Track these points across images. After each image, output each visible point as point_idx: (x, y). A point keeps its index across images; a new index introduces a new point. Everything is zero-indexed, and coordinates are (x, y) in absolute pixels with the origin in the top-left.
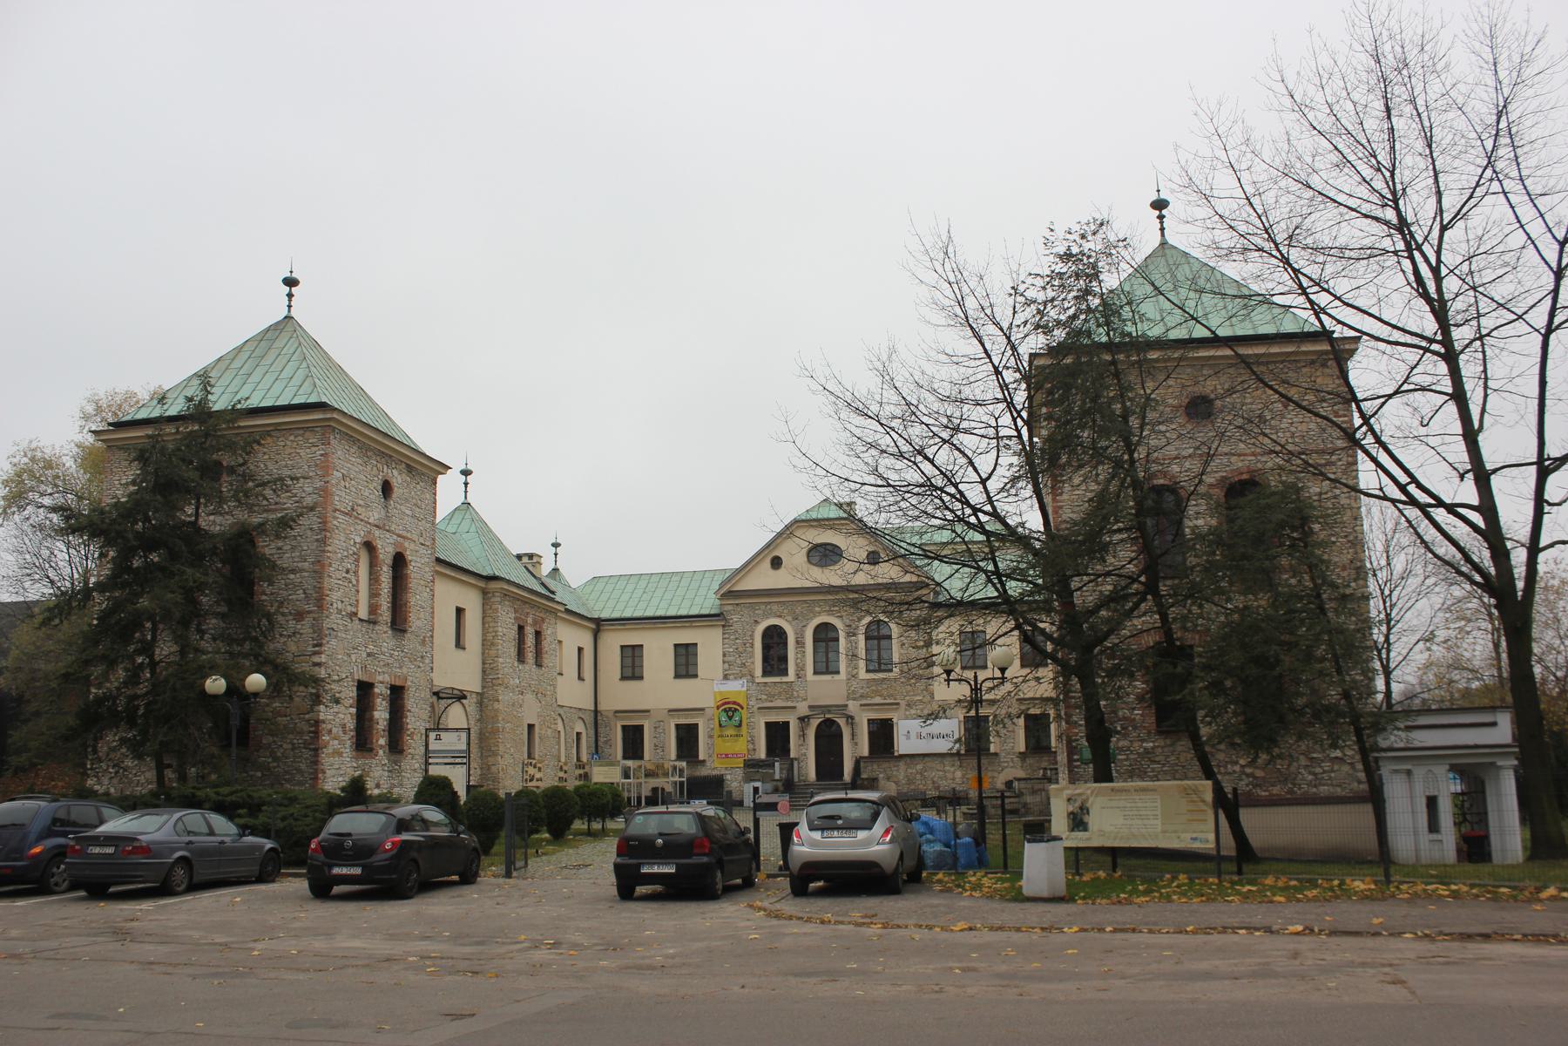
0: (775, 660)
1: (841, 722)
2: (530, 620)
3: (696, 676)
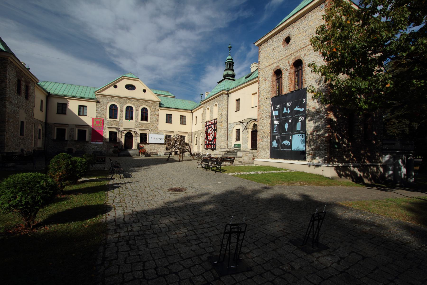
2: (23, 79)
3: (86, 116)
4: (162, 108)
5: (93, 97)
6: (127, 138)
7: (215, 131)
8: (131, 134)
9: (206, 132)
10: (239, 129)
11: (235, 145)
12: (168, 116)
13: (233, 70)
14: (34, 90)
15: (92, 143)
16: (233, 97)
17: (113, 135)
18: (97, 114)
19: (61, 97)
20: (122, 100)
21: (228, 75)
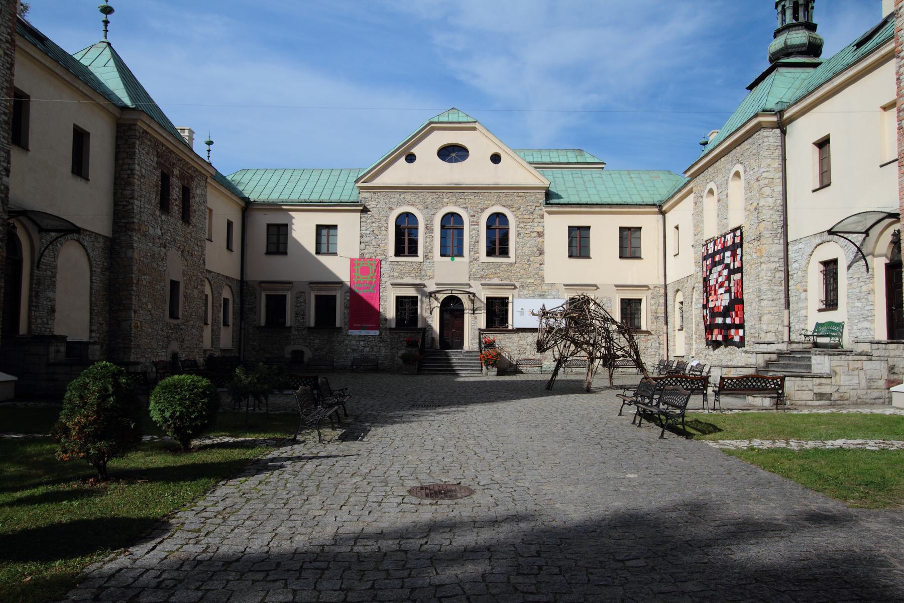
0: (406, 243)
1: (464, 299)
2: (176, 172)
3: (335, 254)
4: (555, 209)
5: (352, 199)
6: (447, 316)
7: (737, 276)
8: (458, 301)
9: (706, 280)
10: (835, 262)
11: (818, 325)
12: (576, 233)
13: (812, 27)
14: (204, 196)
15: (351, 332)
16: (803, 133)
17: (406, 305)
18: (363, 245)
19: (274, 207)
20: (430, 198)
21: (787, 51)
